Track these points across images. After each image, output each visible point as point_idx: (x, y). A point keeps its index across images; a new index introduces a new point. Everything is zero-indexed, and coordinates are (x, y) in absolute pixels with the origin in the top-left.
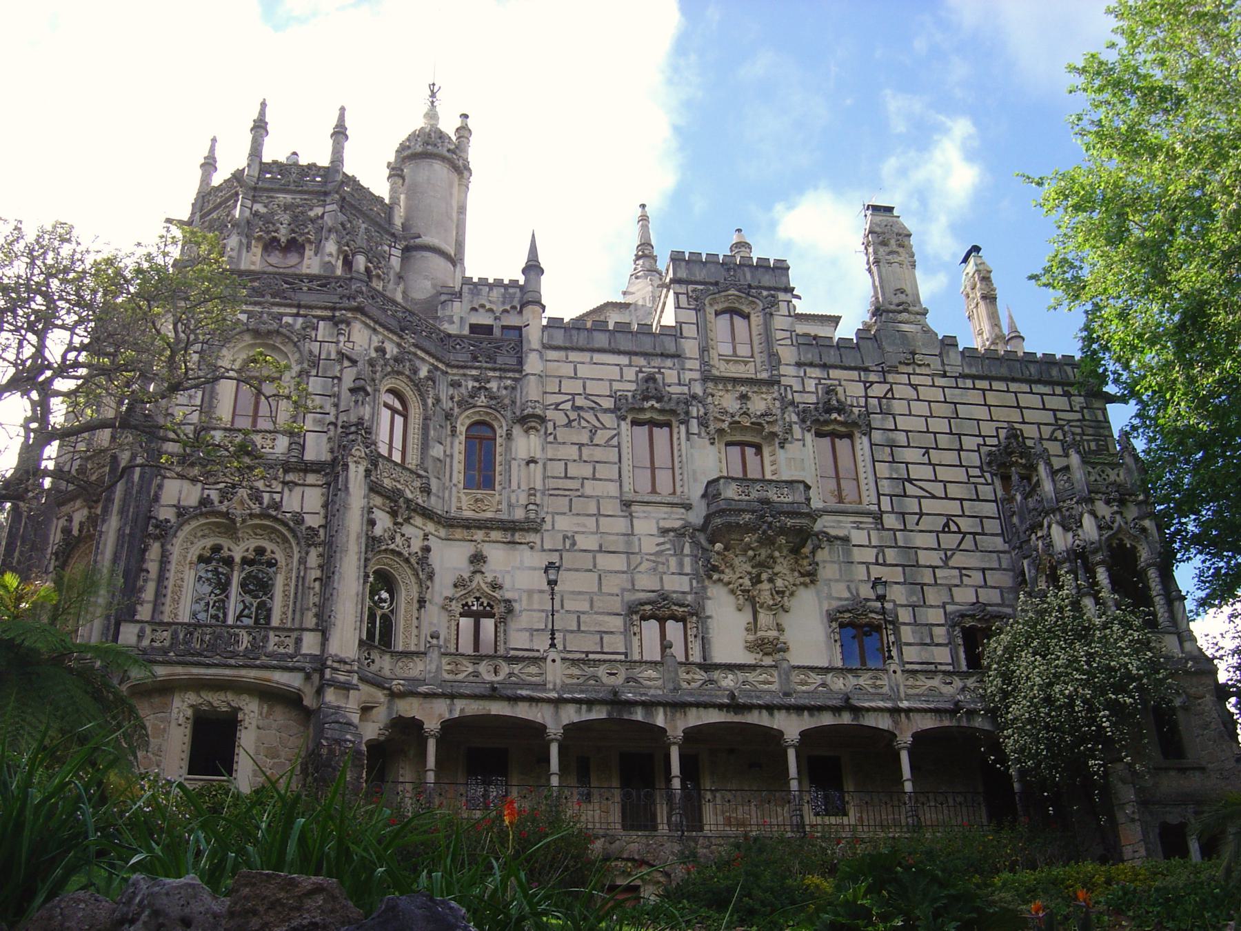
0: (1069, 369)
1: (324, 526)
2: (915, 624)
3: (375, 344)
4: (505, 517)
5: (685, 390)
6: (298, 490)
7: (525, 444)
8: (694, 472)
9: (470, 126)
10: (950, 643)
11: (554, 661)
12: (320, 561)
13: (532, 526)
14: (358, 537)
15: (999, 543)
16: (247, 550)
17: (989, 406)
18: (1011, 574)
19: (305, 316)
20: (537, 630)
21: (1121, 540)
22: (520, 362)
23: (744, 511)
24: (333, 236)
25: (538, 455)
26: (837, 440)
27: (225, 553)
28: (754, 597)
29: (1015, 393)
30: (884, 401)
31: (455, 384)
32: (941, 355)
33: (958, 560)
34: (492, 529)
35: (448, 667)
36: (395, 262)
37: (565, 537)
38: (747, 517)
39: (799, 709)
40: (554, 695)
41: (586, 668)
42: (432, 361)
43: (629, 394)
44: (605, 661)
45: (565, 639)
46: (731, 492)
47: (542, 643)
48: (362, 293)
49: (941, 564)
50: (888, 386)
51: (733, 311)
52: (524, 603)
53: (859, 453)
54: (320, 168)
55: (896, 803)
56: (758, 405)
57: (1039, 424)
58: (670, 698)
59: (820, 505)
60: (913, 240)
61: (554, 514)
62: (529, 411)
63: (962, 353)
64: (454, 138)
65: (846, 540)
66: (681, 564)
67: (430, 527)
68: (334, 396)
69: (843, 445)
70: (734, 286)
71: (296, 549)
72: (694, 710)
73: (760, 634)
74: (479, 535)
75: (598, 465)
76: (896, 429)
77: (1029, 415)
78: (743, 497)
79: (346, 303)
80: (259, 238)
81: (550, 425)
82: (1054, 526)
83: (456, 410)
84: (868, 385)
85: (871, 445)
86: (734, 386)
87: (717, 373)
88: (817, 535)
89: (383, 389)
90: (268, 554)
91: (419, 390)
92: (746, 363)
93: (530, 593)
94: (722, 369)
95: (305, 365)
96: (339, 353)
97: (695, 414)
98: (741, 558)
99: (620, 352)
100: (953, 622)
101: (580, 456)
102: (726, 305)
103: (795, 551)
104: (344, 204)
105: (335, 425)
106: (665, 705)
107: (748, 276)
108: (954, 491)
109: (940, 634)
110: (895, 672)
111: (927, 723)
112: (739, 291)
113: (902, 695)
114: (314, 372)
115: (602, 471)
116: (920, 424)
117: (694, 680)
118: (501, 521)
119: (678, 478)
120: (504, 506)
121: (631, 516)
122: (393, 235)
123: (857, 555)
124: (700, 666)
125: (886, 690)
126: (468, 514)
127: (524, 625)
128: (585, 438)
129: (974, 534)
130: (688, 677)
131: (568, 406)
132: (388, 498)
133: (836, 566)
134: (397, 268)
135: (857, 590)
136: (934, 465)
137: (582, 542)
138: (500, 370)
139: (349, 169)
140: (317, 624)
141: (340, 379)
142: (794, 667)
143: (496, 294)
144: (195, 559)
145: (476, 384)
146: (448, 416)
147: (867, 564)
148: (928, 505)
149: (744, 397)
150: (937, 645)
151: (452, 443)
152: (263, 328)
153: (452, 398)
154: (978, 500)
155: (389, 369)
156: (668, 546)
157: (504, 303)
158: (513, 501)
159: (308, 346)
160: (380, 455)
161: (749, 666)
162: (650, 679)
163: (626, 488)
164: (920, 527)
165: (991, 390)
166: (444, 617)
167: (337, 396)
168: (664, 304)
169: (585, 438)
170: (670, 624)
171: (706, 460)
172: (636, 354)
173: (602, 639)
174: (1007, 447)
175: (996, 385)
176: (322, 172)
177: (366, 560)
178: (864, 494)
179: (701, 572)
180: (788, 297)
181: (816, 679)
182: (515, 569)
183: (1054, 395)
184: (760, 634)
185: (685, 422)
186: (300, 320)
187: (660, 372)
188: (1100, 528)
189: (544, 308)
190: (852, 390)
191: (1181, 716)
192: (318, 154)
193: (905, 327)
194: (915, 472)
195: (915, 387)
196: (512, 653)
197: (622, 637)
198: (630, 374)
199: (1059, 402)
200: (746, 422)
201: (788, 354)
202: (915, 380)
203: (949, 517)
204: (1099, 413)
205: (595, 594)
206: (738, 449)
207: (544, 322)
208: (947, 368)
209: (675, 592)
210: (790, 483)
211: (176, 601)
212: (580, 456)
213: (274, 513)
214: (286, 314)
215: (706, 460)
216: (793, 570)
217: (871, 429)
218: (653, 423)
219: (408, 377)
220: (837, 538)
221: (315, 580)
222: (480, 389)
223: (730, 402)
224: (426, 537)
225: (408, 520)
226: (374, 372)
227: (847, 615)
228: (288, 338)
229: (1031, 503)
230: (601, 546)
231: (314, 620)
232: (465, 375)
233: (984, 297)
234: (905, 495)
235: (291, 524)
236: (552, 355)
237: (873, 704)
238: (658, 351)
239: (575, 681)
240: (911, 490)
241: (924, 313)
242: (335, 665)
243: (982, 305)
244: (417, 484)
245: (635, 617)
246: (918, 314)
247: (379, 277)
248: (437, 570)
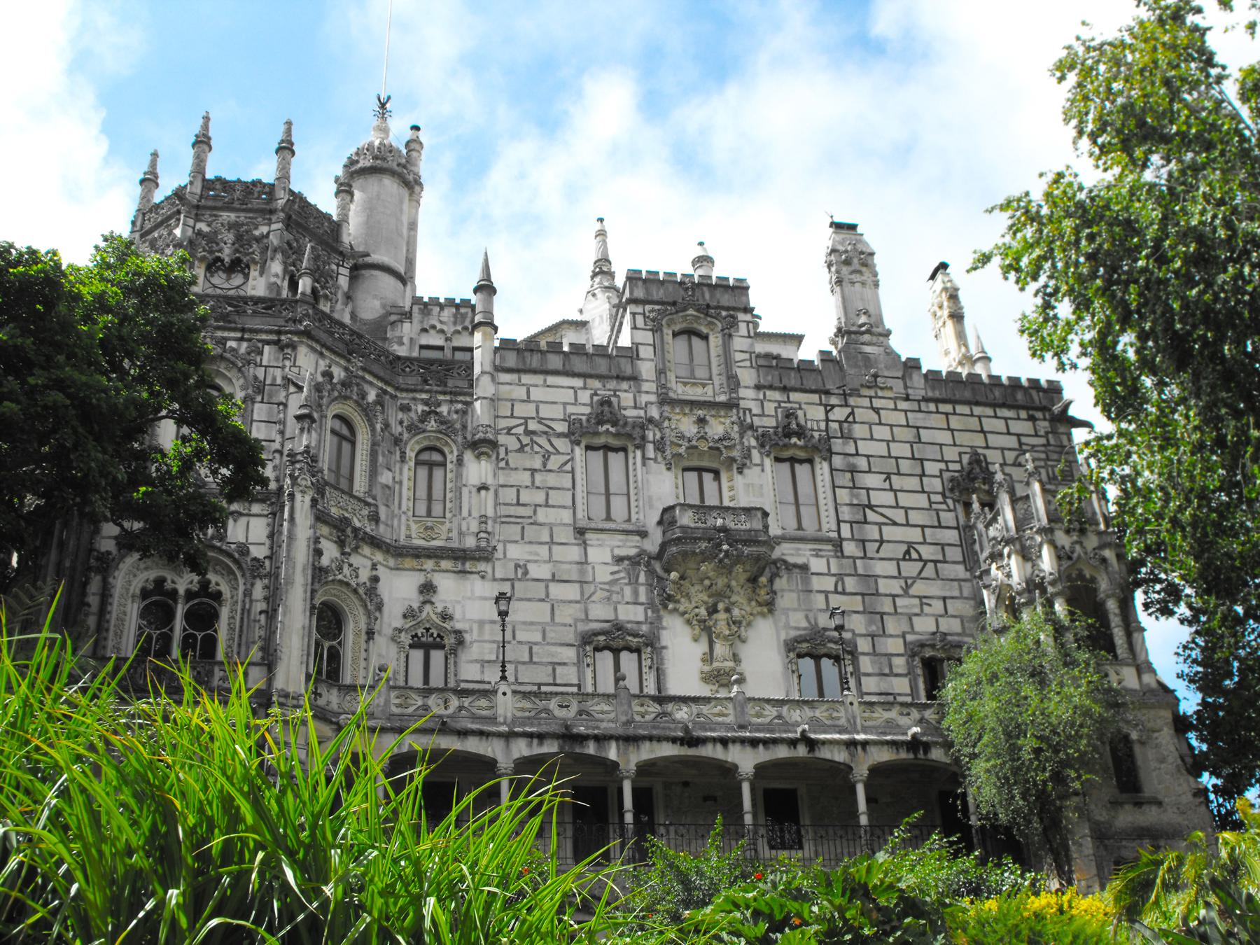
0: (1034, 393)
1: (270, 558)
2: (874, 653)
4: (455, 545)
5: (642, 413)
6: (243, 520)
7: (477, 470)
8: (650, 498)
9: (422, 139)
10: (909, 673)
11: (504, 694)
12: (266, 593)
13: (484, 554)
14: (304, 569)
15: (960, 571)
16: (191, 582)
17: (952, 430)
18: (972, 602)
19: (249, 340)
20: (489, 662)
21: (1080, 571)
22: (471, 386)
23: (700, 539)
24: (279, 256)
25: (490, 481)
26: (797, 466)
27: (168, 585)
28: (710, 628)
29: (979, 417)
30: (845, 425)
31: (405, 409)
32: (903, 378)
33: (919, 588)
34: (442, 558)
35: (397, 701)
36: (343, 281)
37: (517, 566)
38: (704, 545)
39: (754, 743)
40: (504, 728)
41: (537, 701)
42: (380, 384)
43: (584, 418)
44: (557, 694)
45: (516, 670)
46: (686, 519)
47: (493, 675)
48: (307, 315)
49: (900, 592)
50: (849, 410)
51: (690, 333)
52: (475, 636)
53: (819, 478)
54: (264, 185)
55: (850, 837)
56: (716, 428)
57: (1003, 449)
58: (621, 731)
59: (779, 532)
60: (877, 259)
61: (505, 542)
62: (480, 435)
63: (926, 376)
64: (404, 151)
65: (804, 568)
66: (636, 593)
67: (379, 557)
68: (280, 422)
69: (802, 471)
70: (693, 306)
71: (241, 581)
72: (647, 744)
73: (715, 665)
74: (429, 564)
75: (551, 492)
76: (857, 454)
77: (993, 440)
78: (700, 525)
79: (291, 327)
80: (202, 259)
81: (502, 451)
82: (1013, 557)
83: (406, 436)
84: (829, 408)
85: (832, 470)
86: (691, 410)
87: (672, 395)
88: (775, 562)
89: (330, 414)
90: (212, 588)
91: (367, 415)
92: (704, 386)
93: (481, 623)
94: (680, 391)
95: (250, 391)
96: (284, 378)
97: (651, 437)
98: (697, 587)
100: (913, 651)
101: (533, 482)
102: (684, 325)
103: (753, 580)
104: (289, 223)
105: (281, 453)
106: (617, 738)
107: (707, 296)
108: (915, 517)
109: (900, 664)
110: (851, 704)
111: (884, 756)
112: (698, 310)
113: (859, 727)
114: (259, 398)
115: (555, 498)
116: (881, 449)
117: (647, 713)
118: (451, 549)
119: (633, 504)
120: (454, 534)
121: (585, 544)
122: (341, 253)
123: (817, 583)
124: (654, 698)
125: (843, 722)
126: (418, 542)
127: (475, 657)
128: (537, 464)
129: (935, 562)
130: (642, 709)
131: (520, 430)
132: (335, 527)
133: (794, 595)
135: (816, 619)
136: (895, 491)
137: (534, 571)
138: (451, 393)
140: (263, 658)
141: (285, 405)
142: (749, 699)
143: (448, 314)
144: (138, 592)
145: (426, 408)
146: (397, 441)
147: (826, 593)
149: (701, 421)
150: (897, 675)
151: (401, 470)
153: (401, 423)
154: (940, 526)
155: (336, 394)
156: (622, 575)
157: (455, 323)
158: (464, 528)
159: (252, 370)
160: (327, 483)
161: (704, 698)
162: (602, 712)
163: (580, 515)
164: (882, 554)
165: (955, 413)
166: (393, 649)
167: (283, 422)
168: (621, 324)
169: (537, 464)
170: (625, 656)
171: (661, 486)
172: (591, 376)
173: (554, 670)
174: (970, 472)
175: (959, 409)
176: (267, 189)
177: (313, 592)
178: (824, 520)
179: (657, 601)
180: (748, 317)
181: (771, 712)
182: (466, 599)
183: (1019, 419)
184: (715, 665)
185: (641, 447)
186: (245, 345)
187: (615, 395)
188: (1059, 558)
189: (496, 329)
190: (812, 413)
191: (1137, 749)
192: (266, 171)
193: (868, 349)
194: (877, 498)
195: (877, 411)
196: (463, 685)
197: (575, 669)
198: (585, 397)
199: (1023, 427)
200: (704, 446)
201: (747, 376)
202: (877, 403)
203: (910, 545)
204: (1064, 438)
205: (547, 623)
206: (695, 474)
207: (497, 344)
208: (910, 391)
209: (629, 622)
210: (748, 511)
211: (119, 635)
212: (533, 482)
213: (219, 544)
214: (230, 339)
215: (661, 486)
216: (750, 600)
217: (832, 453)
218: (607, 448)
219: (356, 402)
220: (795, 566)
221: (261, 613)
222: (430, 413)
224: (374, 567)
225: (356, 549)
226: (321, 398)
227: (805, 645)
228: (233, 363)
229: (992, 532)
230: (553, 575)
231: (260, 654)
232: (414, 399)
233: (952, 316)
234: (866, 522)
235: (237, 555)
237: (829, 736)
238: (614, 373)
239: (527, 714)
240: (871, 516)
241: (887, 334)
242: (282, 700)
243: (950, 323)
244: (365, 512)
245: (588, 648)
246: (880, 335)
247: (326, 297)
248: (386, 600)
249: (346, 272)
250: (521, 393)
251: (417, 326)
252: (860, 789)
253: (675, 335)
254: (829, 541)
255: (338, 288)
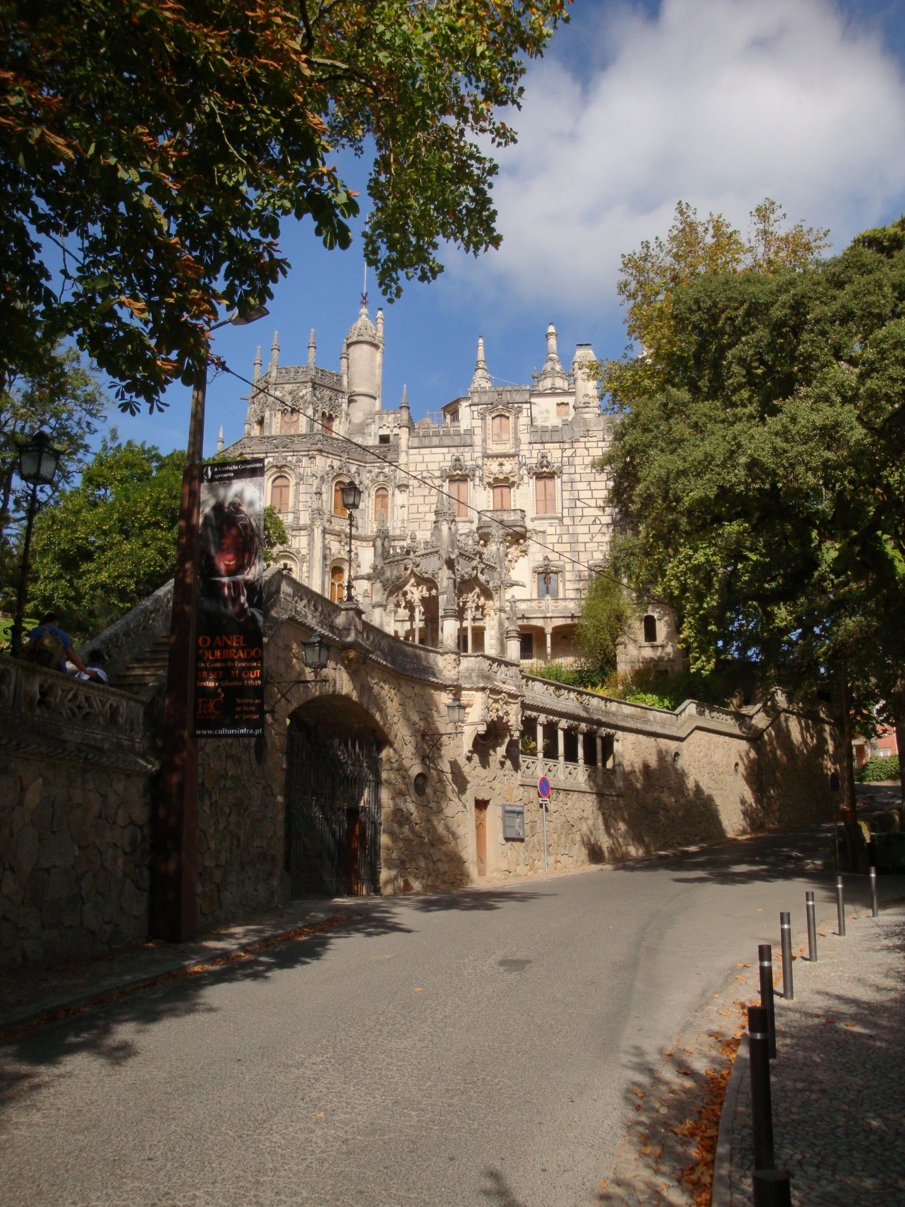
7: (400, 498)
25: (406, 503)
31: (370, 472)
59: (534, 516)
65: (544, 532)
79: (314, 447)
84: (563, 450)
104: (315, 386)
111: (560, 622)
148: (587, 512)
149: (501, 465)
152: (279, 464)
193: (586, 416)
194: (583, 495)
195: (587, 449)
198: (448, 457)
200: (501, 477)
201: (525, 438)
202: (588, 445)
203: (596, 517)
223: (493, 466)
236: (412, 451)
250: (420, 458)
254: (557, 518)
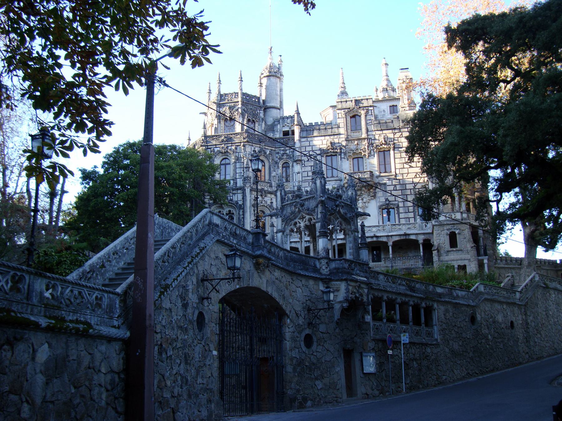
2: (404, 207)
3: (253, 149)
6: (236, 195)
7: (297, 168)
31: (278, 153)
36: (262, 115)
65: (385, 184)
84: (395, 134)
99: (322, 136)
109: (411, 209)
111: (397, 238)
120: (292, 187)
134: (263, 116)
139: (244, 91)
143: (289, 121)
146: (277, 163)
172: (326, 136)
185: (340, 155)
198: (325, 142)
203: (417, 173)
220: (382, 184)
236: (303, 140)
244: (268, 185)
249: (262, 112)
250: (307, 144)
251: (281, 126)
252: (390, 248)
253: (351, 117)
255: (260, 117)
